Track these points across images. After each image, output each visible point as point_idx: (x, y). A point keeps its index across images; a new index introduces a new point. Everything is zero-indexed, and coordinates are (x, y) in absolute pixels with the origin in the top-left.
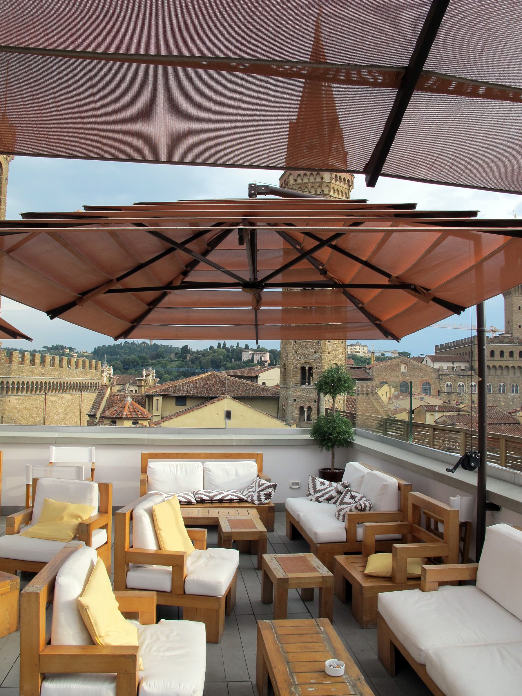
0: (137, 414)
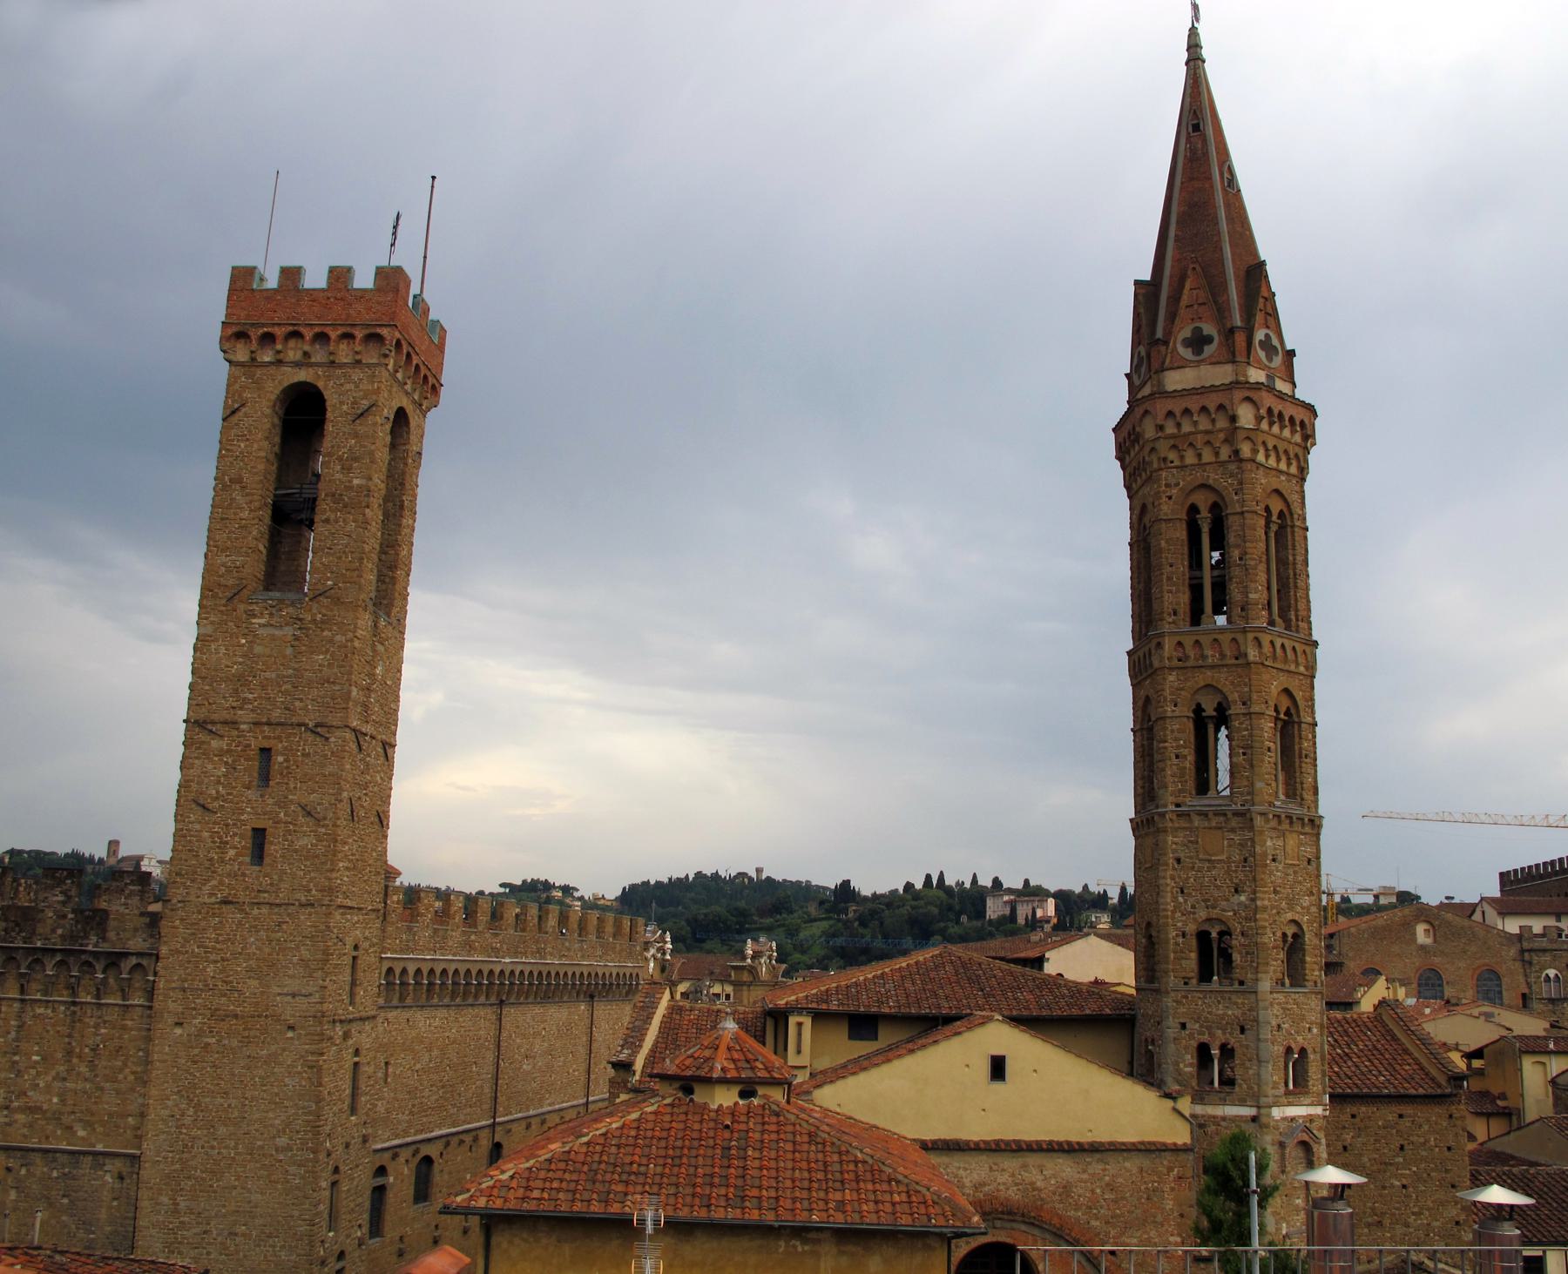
0: (752, 1068)
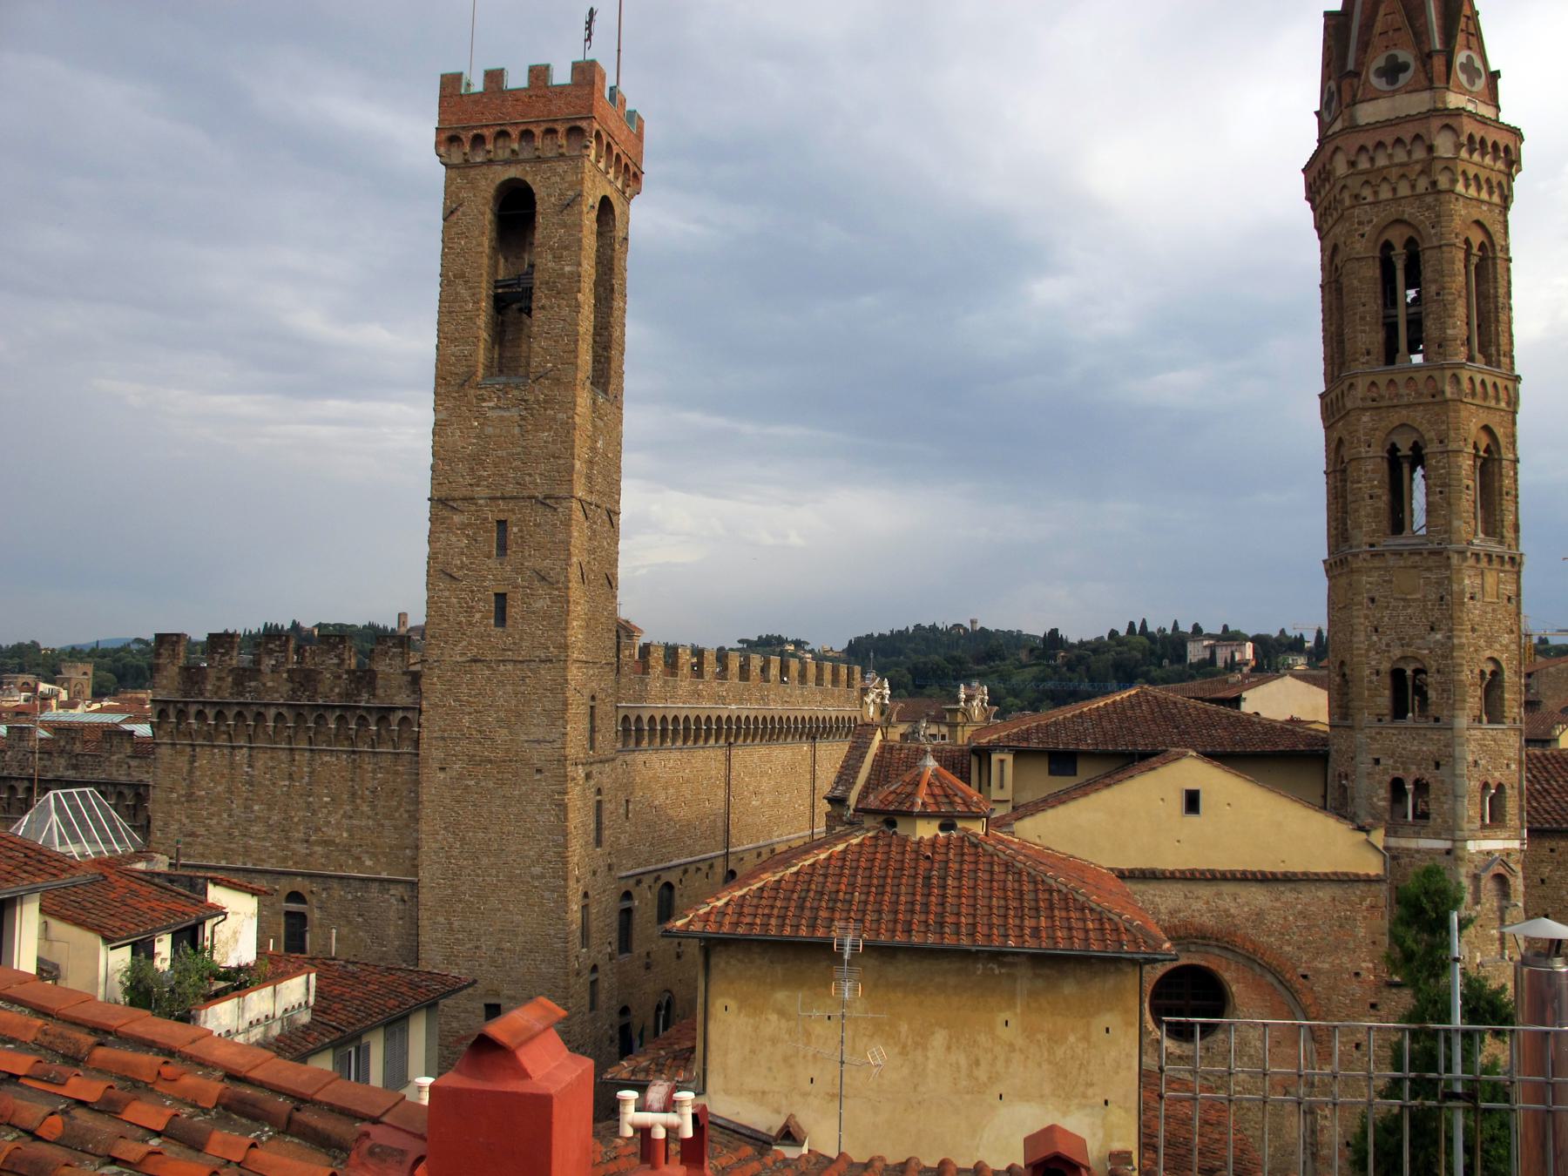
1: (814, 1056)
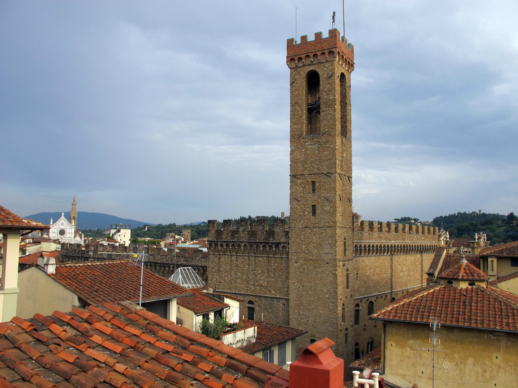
0: (473, 276)
1: (423, 364)
